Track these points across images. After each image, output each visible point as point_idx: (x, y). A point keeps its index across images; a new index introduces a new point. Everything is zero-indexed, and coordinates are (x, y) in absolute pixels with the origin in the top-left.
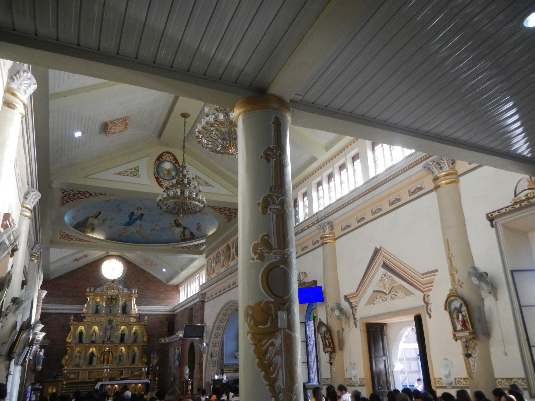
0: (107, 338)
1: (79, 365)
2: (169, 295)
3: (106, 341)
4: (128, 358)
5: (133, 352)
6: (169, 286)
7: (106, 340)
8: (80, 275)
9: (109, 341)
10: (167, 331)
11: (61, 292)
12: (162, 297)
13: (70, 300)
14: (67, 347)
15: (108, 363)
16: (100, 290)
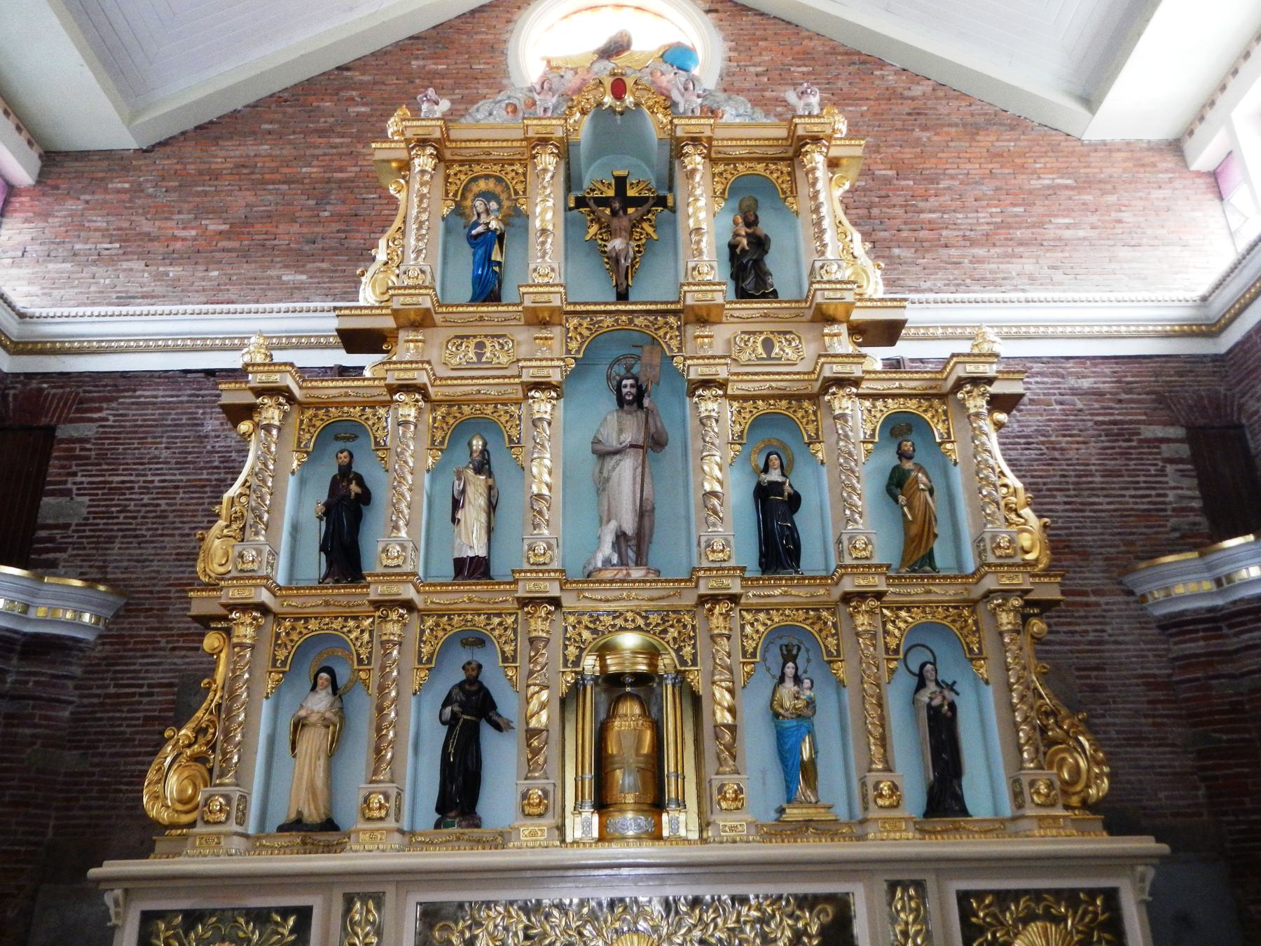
0: (621, 537)
1: (329, 825)
2: (1126, 216)
3: (607, 562)
4: (883, 741)
5: (921, 684)
6: (1105, 147)
7: (607, 549)
8: (363, 109)
9: (638, 563)
10: (1196, 504)
11: (225, 227)
12: (1067, 234)
13: (289, 277)
14: (205, 622)
15: (656, 804)
16: (500, 115)
